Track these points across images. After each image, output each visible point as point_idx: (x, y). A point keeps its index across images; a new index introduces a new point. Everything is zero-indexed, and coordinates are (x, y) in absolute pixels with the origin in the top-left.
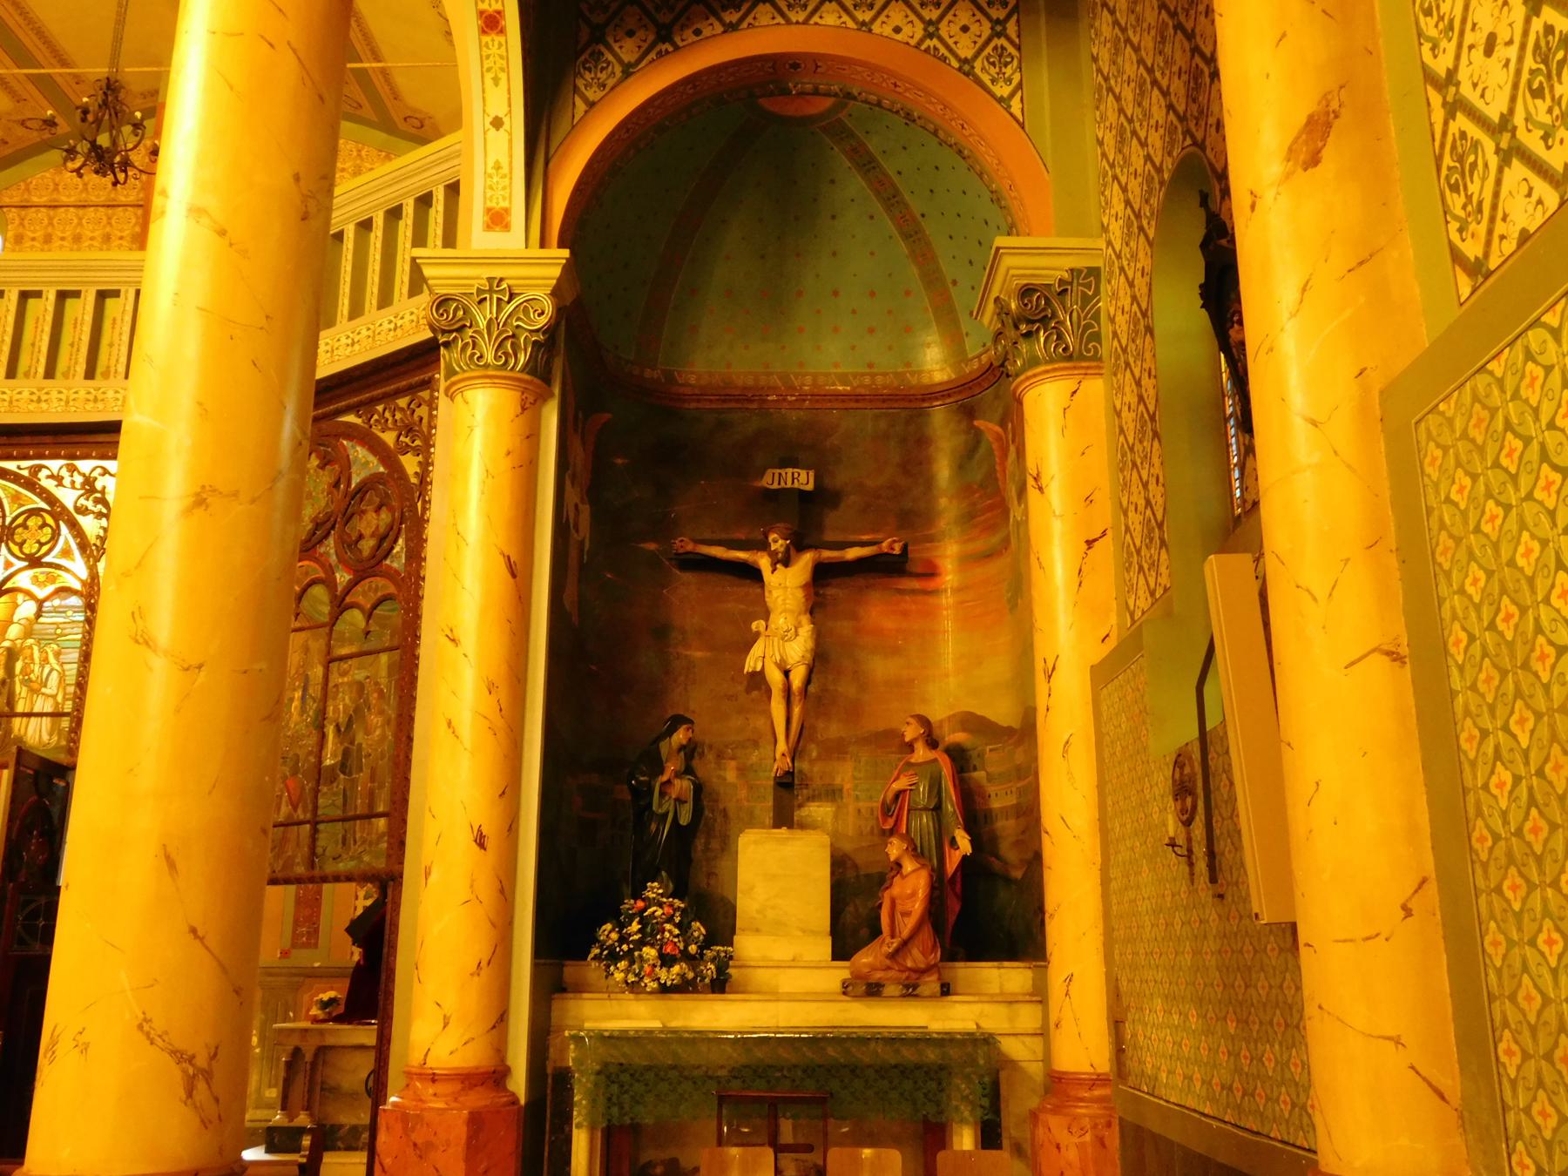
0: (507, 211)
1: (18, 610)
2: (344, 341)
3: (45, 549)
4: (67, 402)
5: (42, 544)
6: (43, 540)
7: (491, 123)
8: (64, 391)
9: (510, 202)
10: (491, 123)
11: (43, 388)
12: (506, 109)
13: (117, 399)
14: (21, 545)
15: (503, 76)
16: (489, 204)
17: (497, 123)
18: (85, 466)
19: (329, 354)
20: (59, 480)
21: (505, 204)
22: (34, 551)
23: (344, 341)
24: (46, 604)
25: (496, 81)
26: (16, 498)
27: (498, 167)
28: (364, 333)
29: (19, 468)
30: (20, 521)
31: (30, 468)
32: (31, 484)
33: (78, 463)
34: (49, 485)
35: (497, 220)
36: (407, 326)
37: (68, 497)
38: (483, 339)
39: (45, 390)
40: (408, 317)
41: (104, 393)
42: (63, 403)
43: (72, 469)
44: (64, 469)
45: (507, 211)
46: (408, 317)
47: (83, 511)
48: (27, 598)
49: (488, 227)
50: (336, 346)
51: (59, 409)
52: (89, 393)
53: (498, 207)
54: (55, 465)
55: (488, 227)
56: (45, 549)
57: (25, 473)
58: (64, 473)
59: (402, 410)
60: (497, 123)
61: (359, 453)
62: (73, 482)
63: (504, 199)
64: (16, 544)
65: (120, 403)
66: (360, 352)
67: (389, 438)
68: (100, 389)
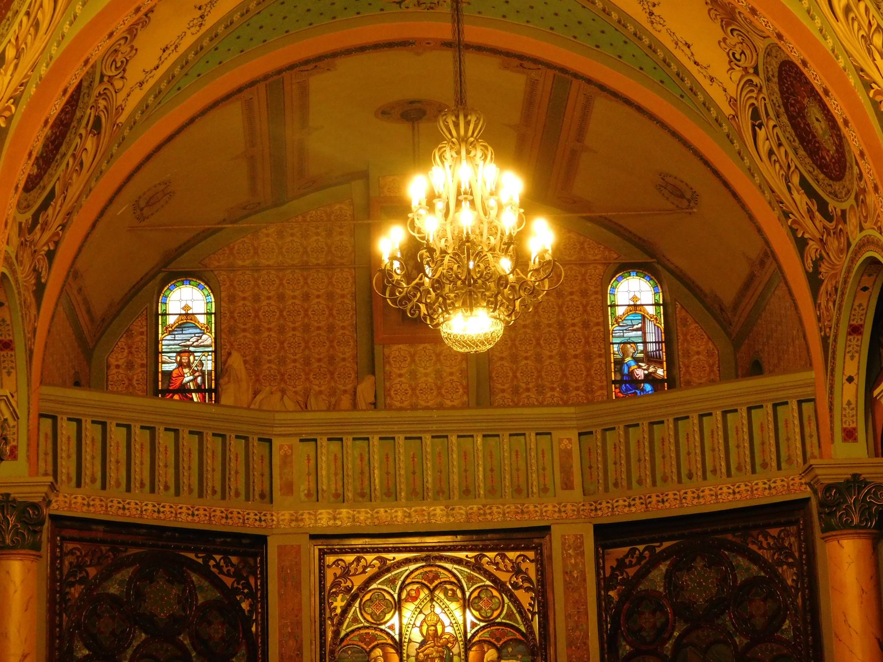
0: (855, 429)
1: (486, 656)
2: (725, 490)
3: (496, 614)
4: (504, 514)
5: (493, 610)
6: (494, 607)
7: (847, 380)
8: (501, 506)
9: (857, 425)
10: (847, 380)
11: (486, 505)
12: (856, 371)
13: (537, 512)
14: (479, 610)
15: (857, 355)
16: (845, 426)
17: (850, 379)
18: (512, 555)
19: (714, 497)
20: (497, 564)
21: (854, 425)
22: (489, 615)
23: (725, 490)
24: (504, 651)
25: (852, 358)
26: (470, 579)
27: (849, 403)
28: (743, 487)
29: (467, 556)
30: (475, 594)
31: (475, 557)
32: (477, 566)
33: (507, 554)
34: (492, 569)
35: (850, 435)
36: (780, 488)
37: (504, 577)
38: (852, 510)
39: (488, 507)
40: (779, 483)
41: (527, 507)
42: (501, 515)
43: (503, 557)
44: (498, 557)
45: (855, 429)
46: (779, 483)
47: (516, 586)
48: (490, 647)
49: (845, 440)
50: (719, 492)
51: (499, 519)
52: (517, 508)
53: (849, 427)
54: (492, 555)
55: (845, 440)
56: (496, 614)
57: (473, 560)
58: (498, 559)
59: (773, 537)
60: (850, 379)
61: (742, 561)
62: (505, 566)
63: (853, 422)
64: (477, 610)
65: (538, 514)
66: (740, 500)
67: (766, 554)
68: (524, 504)
